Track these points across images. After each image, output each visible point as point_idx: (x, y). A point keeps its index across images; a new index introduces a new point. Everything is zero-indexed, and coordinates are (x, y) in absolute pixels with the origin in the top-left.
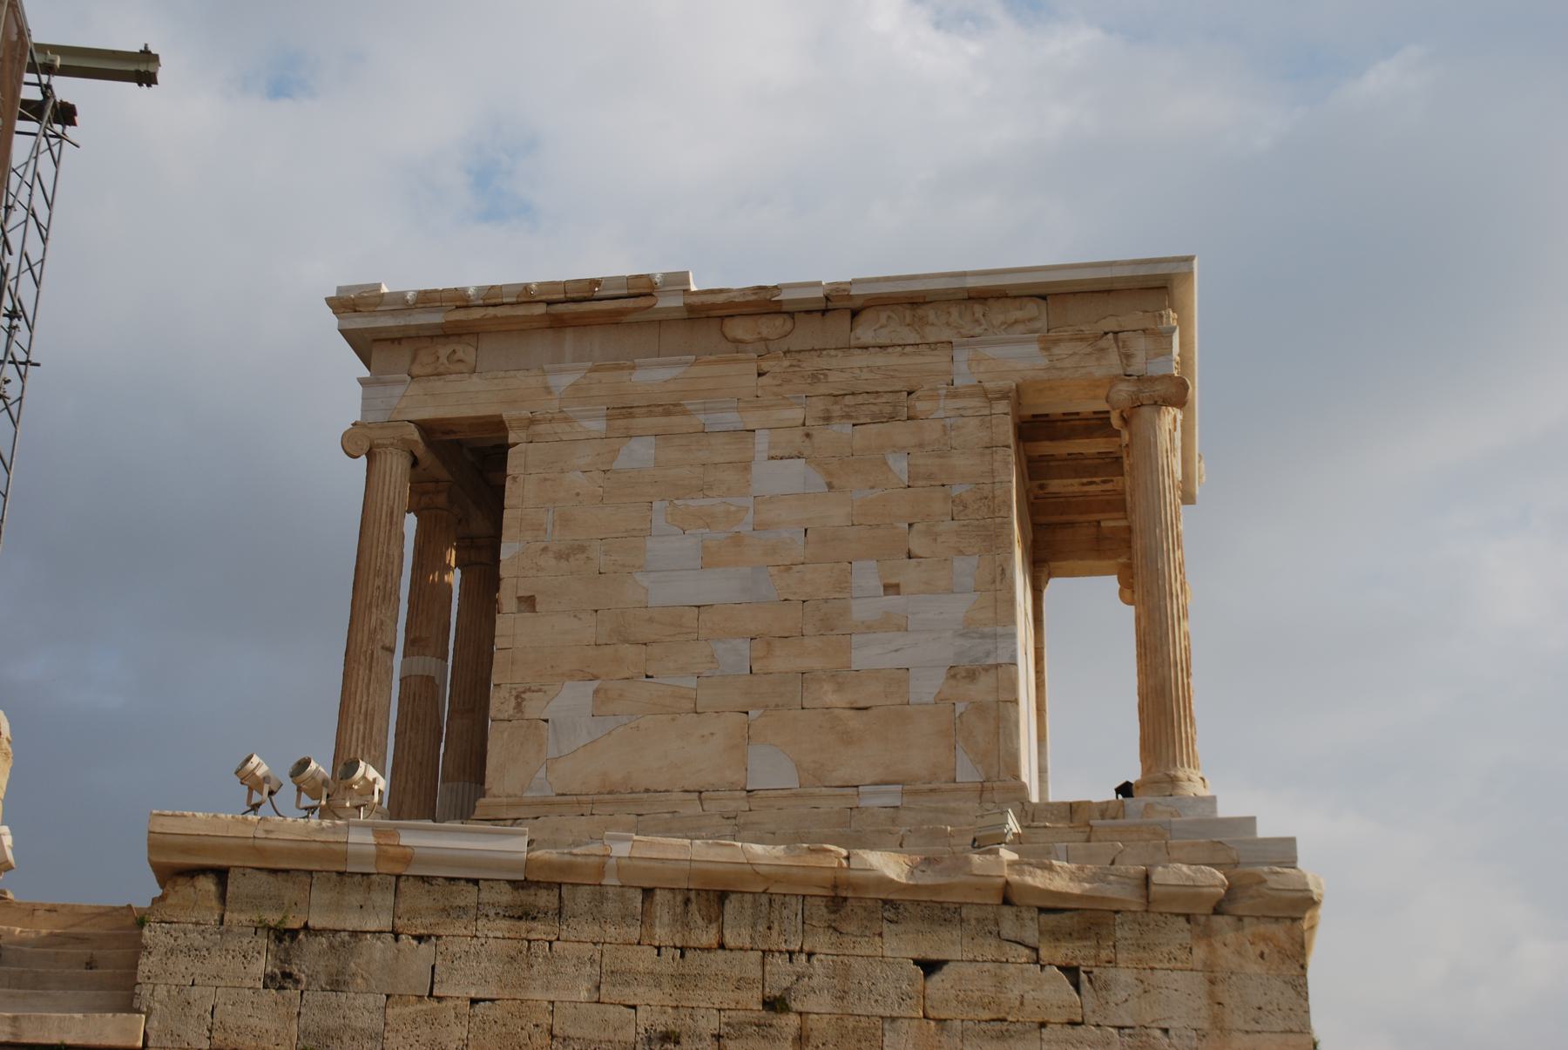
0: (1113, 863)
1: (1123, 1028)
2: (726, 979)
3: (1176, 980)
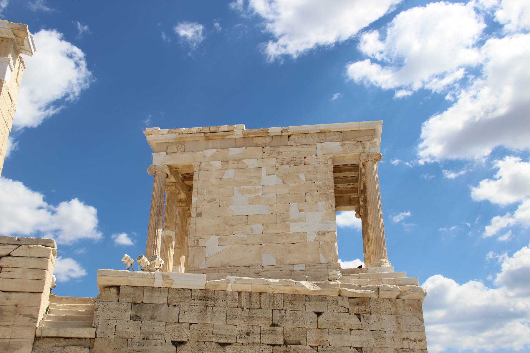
0: (367, 284)
1: (373, 331)
2: (262, 317)
3: (387, 317)
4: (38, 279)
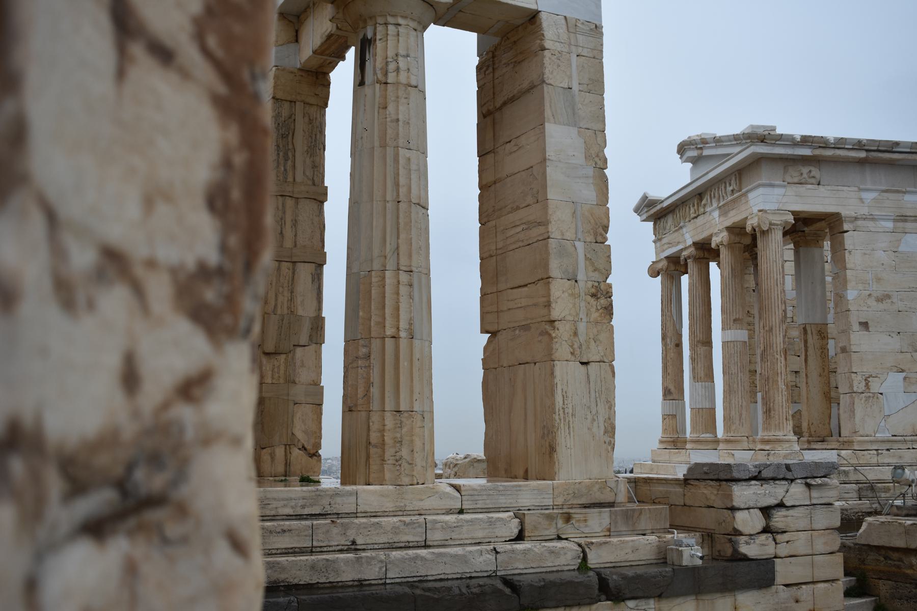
4: (830, 552)
